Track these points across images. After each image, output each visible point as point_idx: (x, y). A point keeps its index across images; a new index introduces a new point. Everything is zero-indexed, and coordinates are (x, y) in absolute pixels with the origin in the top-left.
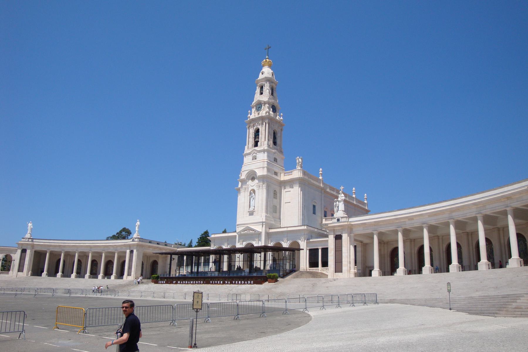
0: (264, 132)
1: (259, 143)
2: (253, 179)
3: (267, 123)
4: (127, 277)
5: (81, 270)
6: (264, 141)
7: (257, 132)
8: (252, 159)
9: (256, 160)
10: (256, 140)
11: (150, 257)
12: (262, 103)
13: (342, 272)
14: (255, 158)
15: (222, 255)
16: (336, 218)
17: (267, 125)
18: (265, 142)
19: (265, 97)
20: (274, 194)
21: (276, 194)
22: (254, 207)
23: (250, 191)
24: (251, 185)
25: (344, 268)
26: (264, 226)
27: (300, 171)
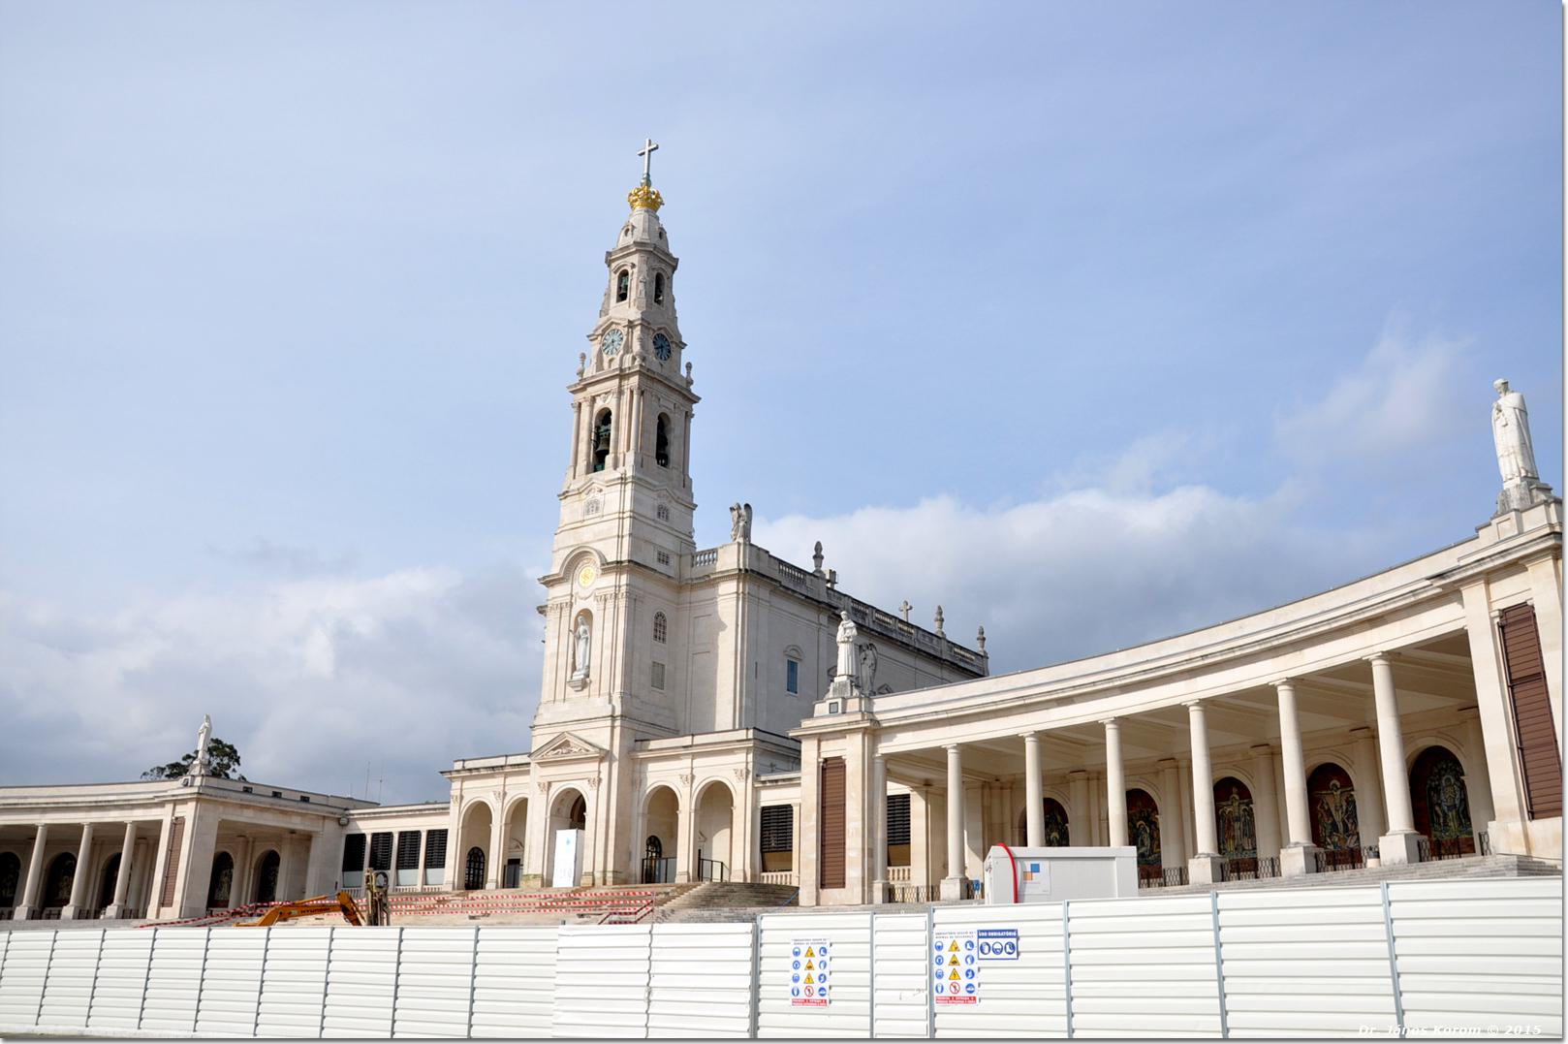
1: (609, 459)
3: (635, 392)
5: (14, 893)
7: (605, 417)
9: (597, 515)
10: (600, 448)
11: (254, 842)
13: (842, 885)
16: (828, 702)
17: (635, 397)
20: (656, 624)
21: (664, 627)
22: (589, 667)
23: (577, 618)
24: (583, 596)
26: (617, 731)
27: (742, 547)
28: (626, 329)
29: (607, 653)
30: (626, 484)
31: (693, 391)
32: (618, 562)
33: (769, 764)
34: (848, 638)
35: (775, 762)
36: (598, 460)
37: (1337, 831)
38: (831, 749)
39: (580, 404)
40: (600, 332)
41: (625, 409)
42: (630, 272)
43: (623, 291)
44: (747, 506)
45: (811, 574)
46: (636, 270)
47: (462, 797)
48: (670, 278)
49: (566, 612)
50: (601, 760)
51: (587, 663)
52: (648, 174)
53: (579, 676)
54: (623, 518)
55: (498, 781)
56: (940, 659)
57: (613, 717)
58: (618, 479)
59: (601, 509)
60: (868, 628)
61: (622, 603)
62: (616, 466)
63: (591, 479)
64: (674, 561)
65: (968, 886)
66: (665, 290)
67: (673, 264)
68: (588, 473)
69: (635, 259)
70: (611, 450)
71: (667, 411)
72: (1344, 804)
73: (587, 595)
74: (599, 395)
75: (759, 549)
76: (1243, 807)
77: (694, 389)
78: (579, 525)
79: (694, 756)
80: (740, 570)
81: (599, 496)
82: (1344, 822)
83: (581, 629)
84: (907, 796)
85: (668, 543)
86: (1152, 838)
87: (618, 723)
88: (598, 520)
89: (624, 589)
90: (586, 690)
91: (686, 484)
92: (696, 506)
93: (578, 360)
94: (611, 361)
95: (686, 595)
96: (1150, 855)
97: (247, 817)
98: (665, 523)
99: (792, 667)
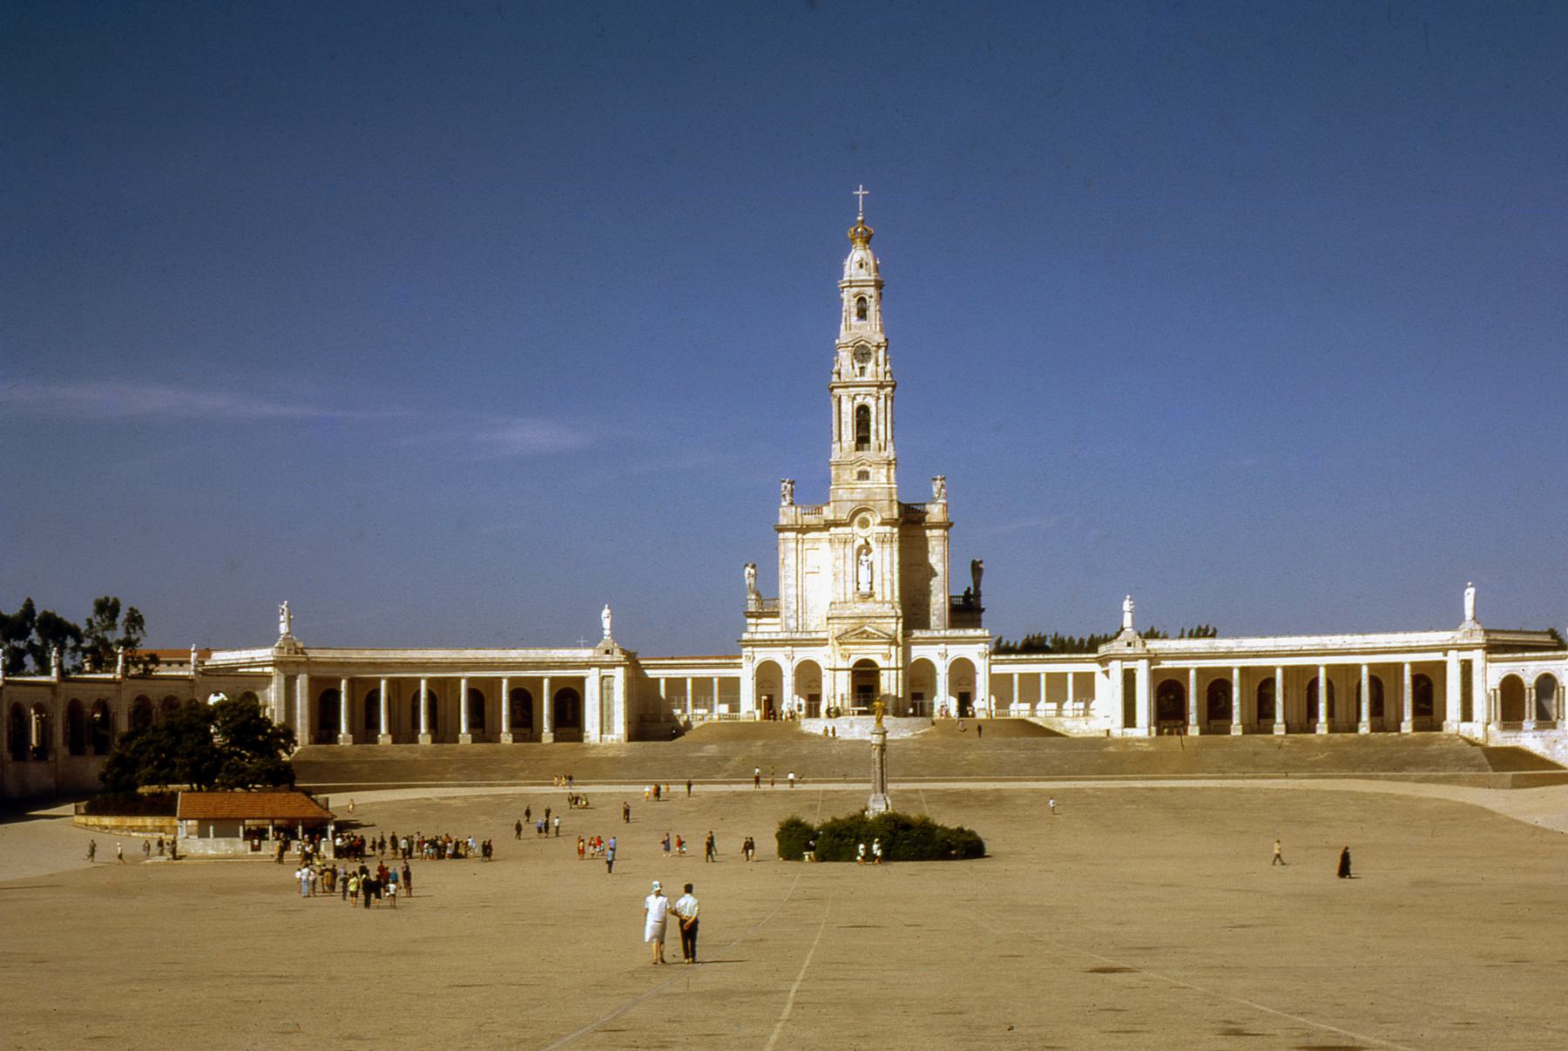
2: (864, 524)
7: (862, 413)
8: (855, 476)
9: (868, 482)
12: (873, 346)
14: (863, 475)
19: (871, 330)
22: (871, 583)
26: (900, 626)
36: (862, 440)
39: (840, 396)
40: (852, 344)
49: (849, 546)
50: (891, 644)
51: (869, 580)
53: (865, 588)
57: (898, 618)
69: (871, 291)
74: (860, 394)
81: (869, 469)
83: (863, 558)
86: (1226, 700)
87: (901, 620)
89: (896, 536)
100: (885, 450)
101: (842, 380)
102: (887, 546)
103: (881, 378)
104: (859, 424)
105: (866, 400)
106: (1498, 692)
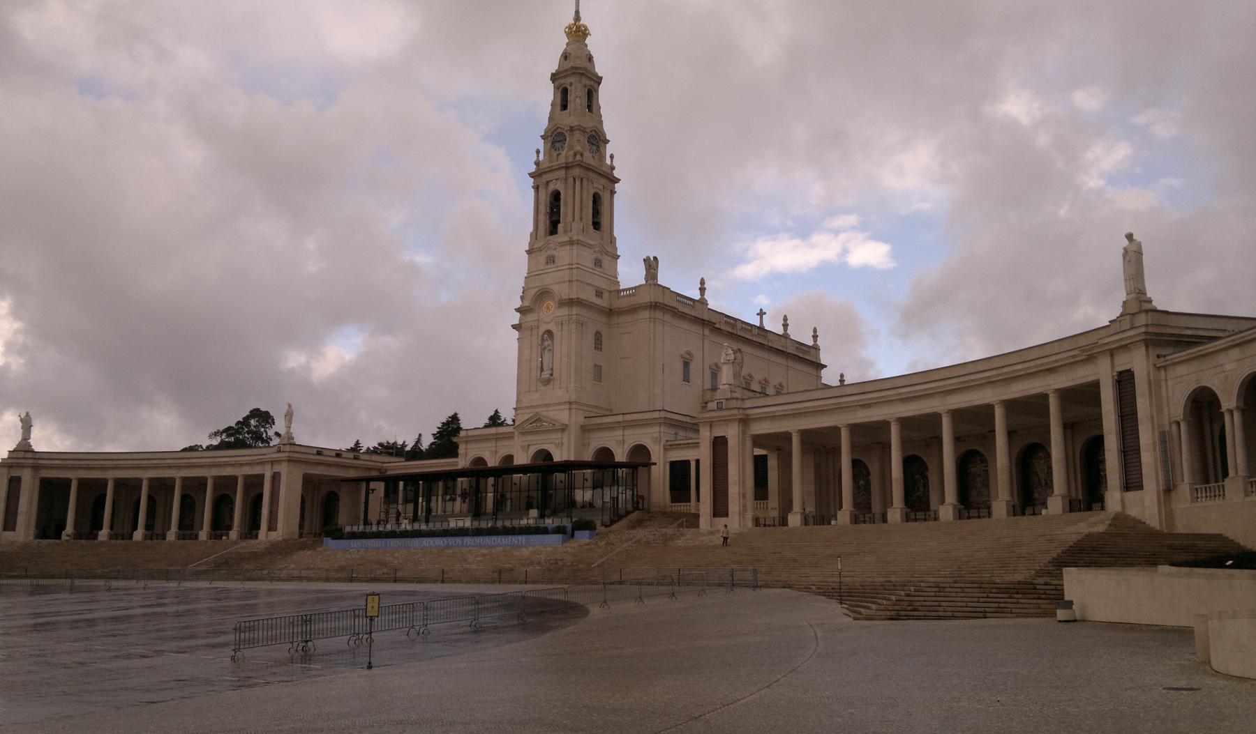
0: (570, 203)
1: (560, 227)
3: (576, 179)
4: (267, 534)
6: (571, 220)
7: (556, 196)
8: (545, 261)
9: (555, 265)
10: (554, 219)
14: (551, 260)
15: (481, 478)
16: (716, 401)
17: (578, 183)
18: (574, 224)
21: (601, 341)
22: (552, 369)
23: (543, 336)
24: (545, 321)
25: (733, 507)
28: (568, 132)
29: (565, 359)
30: (573, 244)
31: (615, 175)
32: (570, 299)
33: (673, 432)
34: (729, 360)
35: (677, 431)
37: (1041, 485)
38: (719, 432)
39: (538, 186)
40: (549, 134)
41: (570, 191)
42: (569, 89)
43: (564, 103)
44: (655, 258)
45: (697, 301)
46: (573, 87)
47: (466, 454)
48: (597, 91)
49: (535, 332)
50: (563, 430)
51: (551, 367)
52: (577, 12)
53: (546, 374)
54: (572, 268)
55: (491, 444)
56: (786, 352)
58: (567, 241)
59: (556, 262)
60: (737, 335)
61: (574, 326)
62: (565, 232)
63: (549, 241)
64: (606, 295)
65: (805, 518)
66: (594, 100)
67: (599, 80)
68: (546, 236)
70: (561, 220)
71: (598, 191)
72: (1046, 469)
73: (549, 320)
75: (664, 287)
76: (983, 468)
77: (616, 174)
78: (541, 272)
79: (624, 428)
80: (651, 303)
81: (554, 253)
82: (1045, 480)
84: (766, 456)
85: (603, 284)
88: (555, 269)
90: (550, 386)
91: (612, 241)
92: (619, 256)
93: (535, 153)
94: (558, 155)
95: (615, 320)
96: (923, 497)
97: (319, 471)
98: (600, 270)
99: (686, 365)
100: (571, 231)
101: (541, 167)
102: (565, 327)
103: (571, 160)
104: (552, 209)
105: (557, 186)
106: (1183, 426)
